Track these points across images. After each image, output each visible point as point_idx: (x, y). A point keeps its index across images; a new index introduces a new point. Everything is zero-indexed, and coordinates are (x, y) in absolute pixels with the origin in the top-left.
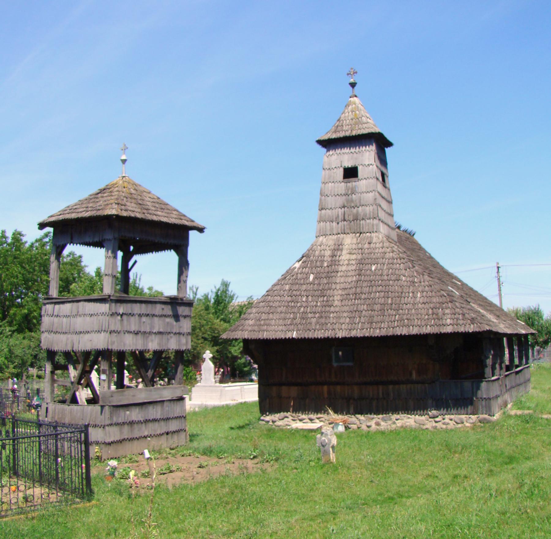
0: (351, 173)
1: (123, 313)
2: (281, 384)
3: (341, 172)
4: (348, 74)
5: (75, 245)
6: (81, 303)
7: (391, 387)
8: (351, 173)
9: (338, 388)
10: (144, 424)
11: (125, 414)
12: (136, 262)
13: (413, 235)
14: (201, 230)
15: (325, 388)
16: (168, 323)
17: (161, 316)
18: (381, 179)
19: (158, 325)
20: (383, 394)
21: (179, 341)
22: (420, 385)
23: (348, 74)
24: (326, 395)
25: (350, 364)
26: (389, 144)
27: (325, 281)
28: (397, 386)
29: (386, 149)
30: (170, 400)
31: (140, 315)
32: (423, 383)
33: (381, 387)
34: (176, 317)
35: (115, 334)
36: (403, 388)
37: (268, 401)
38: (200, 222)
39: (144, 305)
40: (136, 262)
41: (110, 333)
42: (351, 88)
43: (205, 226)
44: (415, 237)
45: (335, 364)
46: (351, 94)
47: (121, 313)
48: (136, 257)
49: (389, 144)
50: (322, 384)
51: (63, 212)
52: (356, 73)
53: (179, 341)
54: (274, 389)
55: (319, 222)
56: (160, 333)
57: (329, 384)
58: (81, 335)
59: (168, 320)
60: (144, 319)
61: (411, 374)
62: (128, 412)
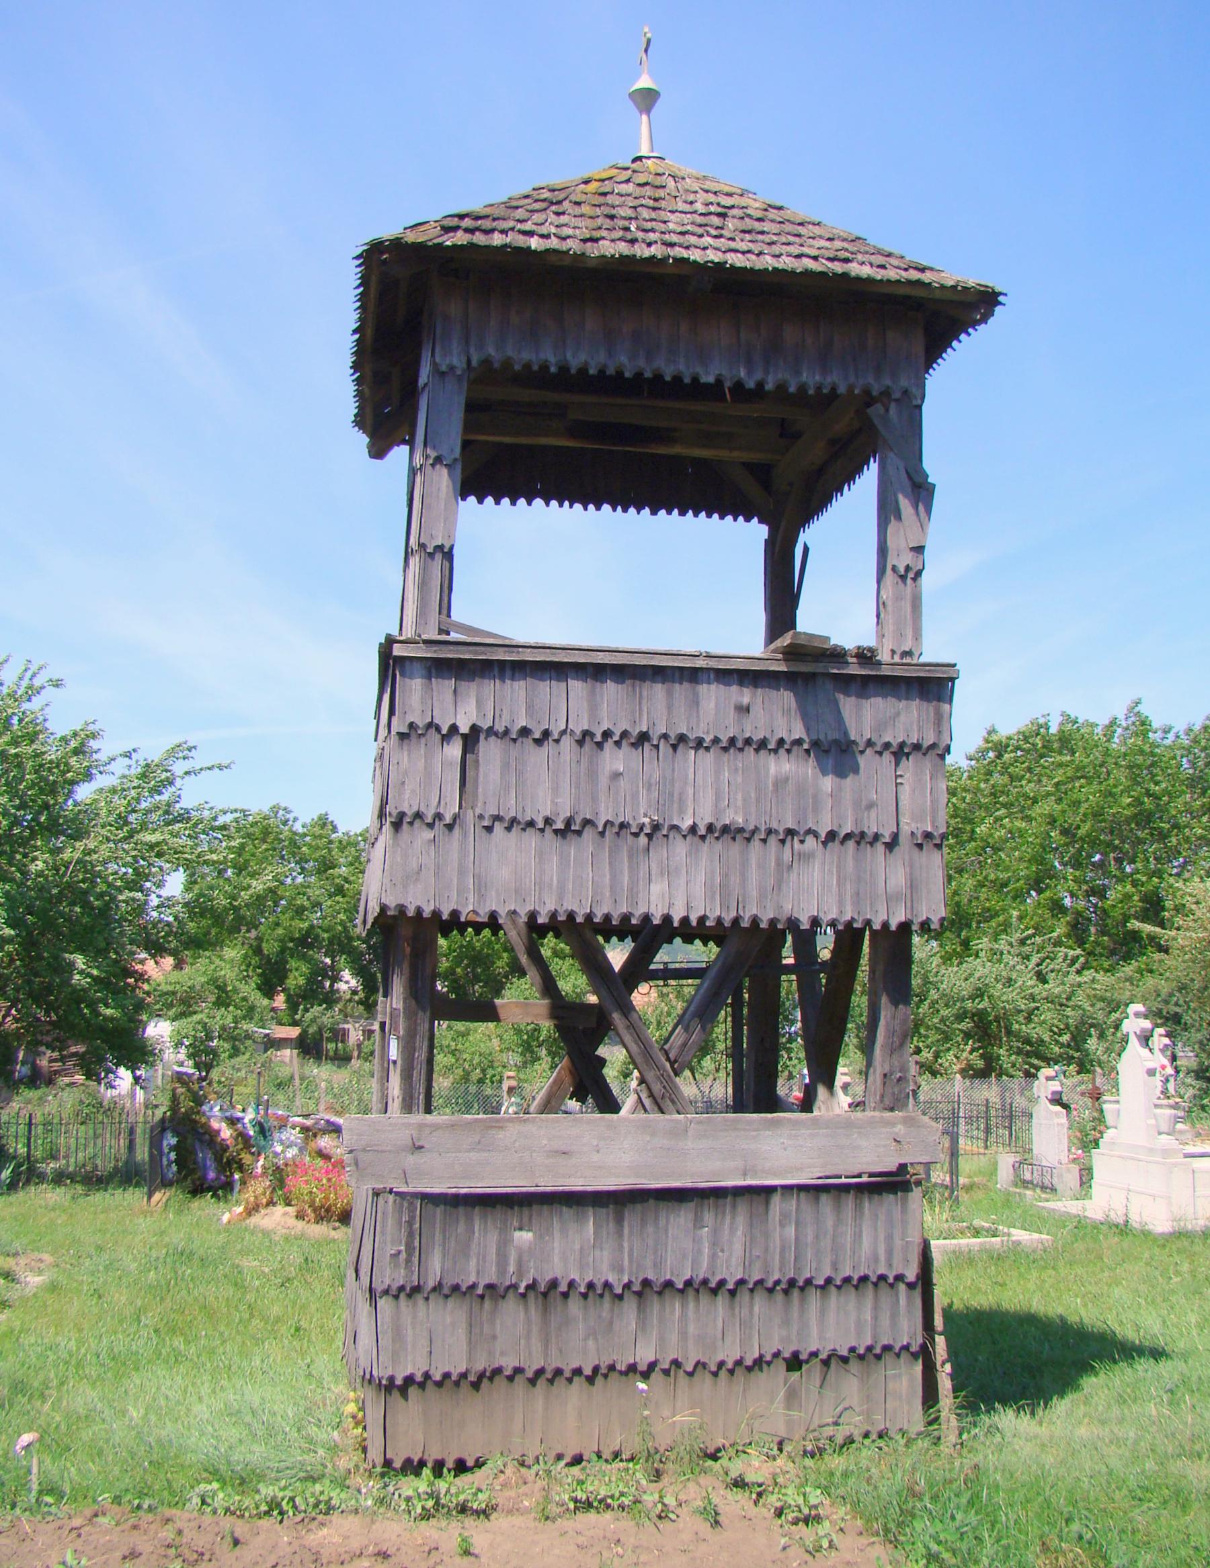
1: (475, 729)
5: (522, 502)
10: (630, 1306)
11: (504, 1244)
12: (806, 550)
16: (781, 783)
19: (707, 789)
30: (814, 1190)
34: (836, 753)
35: (428, 834)
39: (610, 689)
40: (806, 550)
47: (464, 729)
59: (778, 766)
60: (615, 759)
62: (524, 1237)
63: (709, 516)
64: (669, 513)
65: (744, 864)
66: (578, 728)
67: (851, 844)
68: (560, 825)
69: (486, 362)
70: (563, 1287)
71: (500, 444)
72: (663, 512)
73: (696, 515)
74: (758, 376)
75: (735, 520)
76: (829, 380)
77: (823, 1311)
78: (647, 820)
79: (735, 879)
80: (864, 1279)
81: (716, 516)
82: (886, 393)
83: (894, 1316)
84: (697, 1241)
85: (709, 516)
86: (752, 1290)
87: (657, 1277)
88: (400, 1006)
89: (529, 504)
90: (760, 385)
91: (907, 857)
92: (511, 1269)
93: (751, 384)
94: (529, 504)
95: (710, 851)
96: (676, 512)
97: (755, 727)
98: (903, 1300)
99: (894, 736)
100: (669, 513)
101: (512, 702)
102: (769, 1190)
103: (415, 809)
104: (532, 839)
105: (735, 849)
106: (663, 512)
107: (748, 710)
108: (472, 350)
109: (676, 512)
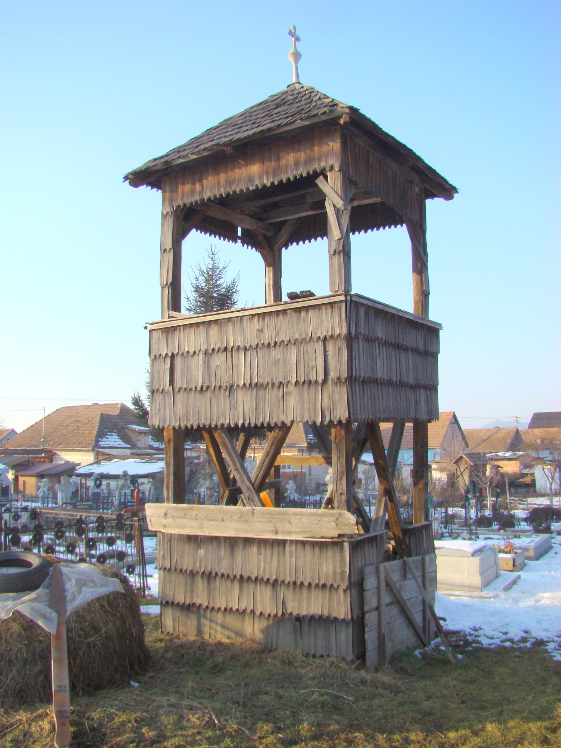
16: (276, 362)
30: (303, 543)
47: (170, 355)
63: (390, 227)
64: (372, 230)
67: (306, 386)
68: (199, 389)
70: (214, 574)
71: (299, 218)
72: (370, 231)
73: (384, 229)
74: (271, 180)
75: (402, 226)
76: (299, 172)
77: (308, 598)
78: (228, 384)
80: (324, 586)
81: (393, 227)
82: (324, 169)
83: (339, 603)
84: (259, 561)
85: (390, 227)
86: (281, 586)
87: (246, 575)
89: (316, 240)
90: (273, 183)
91: (330, 390)
92: (198, 565)
93: (268, 185)
94: (316, 240)
96: (375, 229)
97: (266, 338)
98: (342, 598)
99: (321, 333)
100: (372, 230)
102: (283, 543)
103: (157, 388)
106: (370, 231)
107: (262, 330)
108: (174, 203)
109: (375, 229)
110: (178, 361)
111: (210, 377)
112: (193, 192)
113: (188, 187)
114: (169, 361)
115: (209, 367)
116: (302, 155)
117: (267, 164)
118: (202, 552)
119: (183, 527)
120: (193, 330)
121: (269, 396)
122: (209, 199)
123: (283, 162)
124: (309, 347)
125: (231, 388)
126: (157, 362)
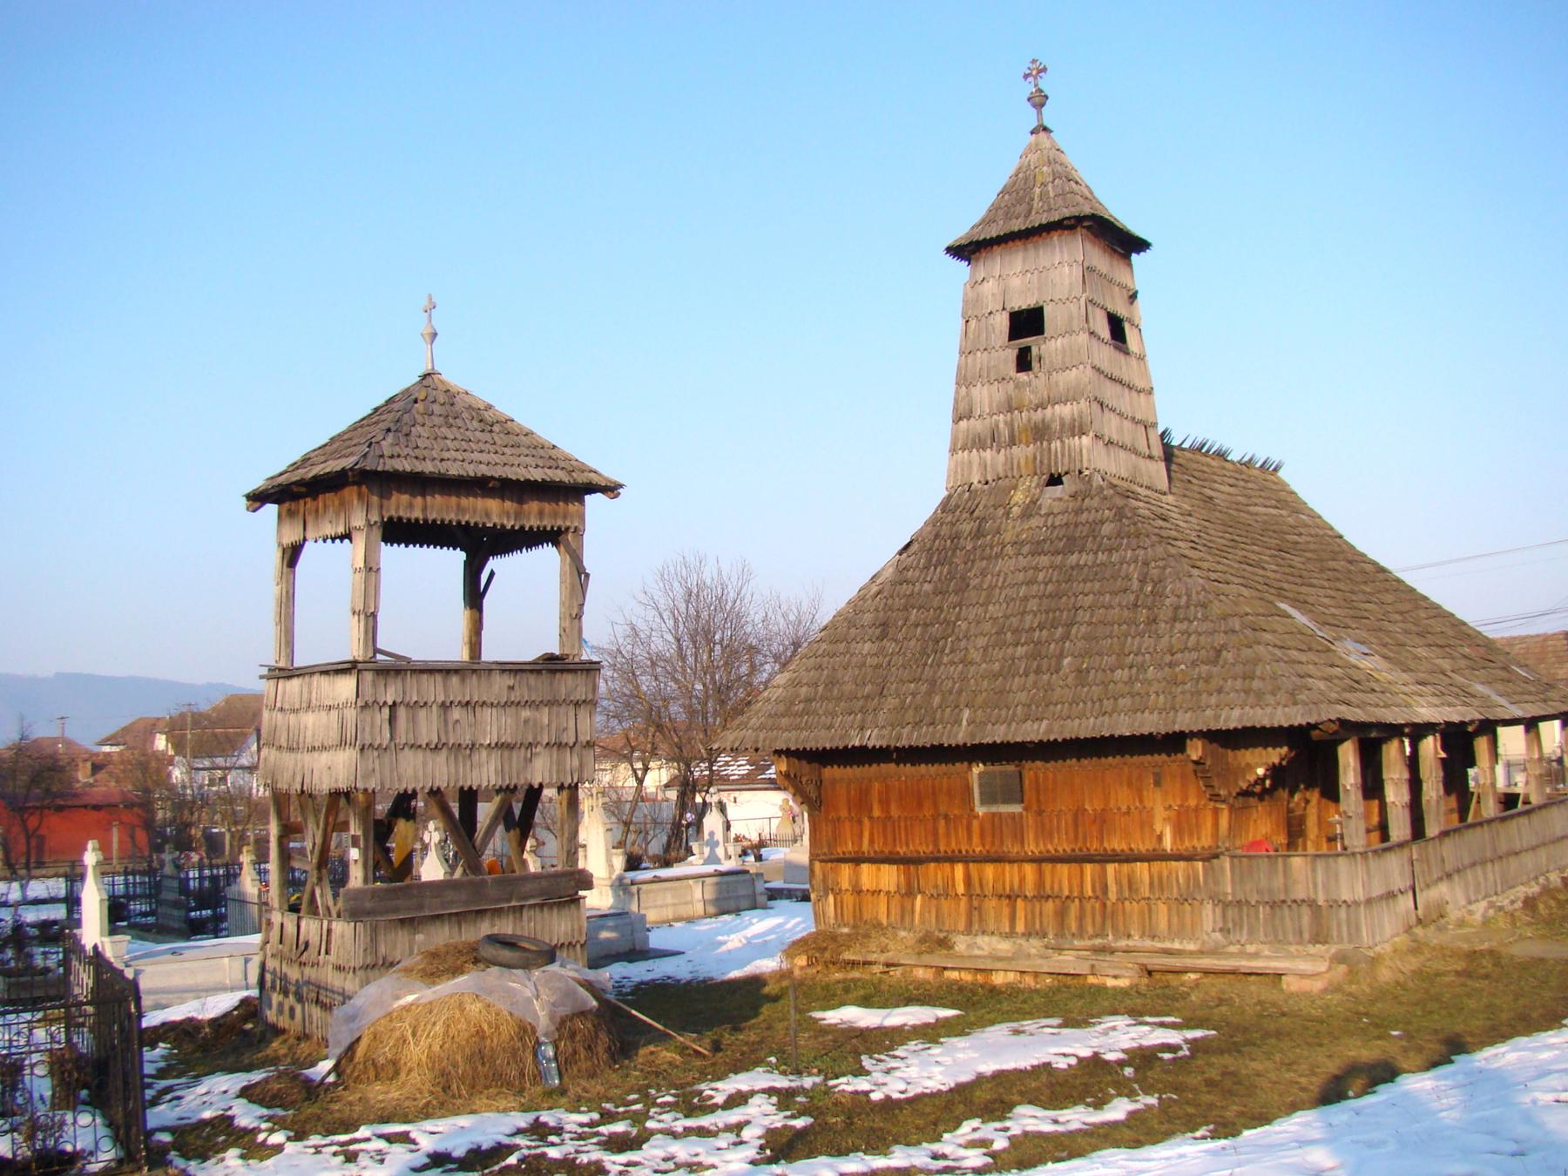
0: (1027, 323)
2: (857, 860)
3: (1002, 322)
4: (1026, 76)
6: (316, 678)
7: (1111, 868)
8: (1027, 323)
9: (989, 870)
12: (492, 574)
13: (1276, 470)
14: (611, 489)
15: (959, 869)
16: (526, 722)
17: (507, 704)
18: (1105, 333)
20: (1094, 890)
21: (560, 763)
22: (1182, 864)
23: (1026, 76)
24: (961, 889)
25: (1016, 809)
26: (1141, 245)
27: (953, 598)
28: (1125, 867)
29: (1134, 256)
31: (445, 707)
32: (1189, 858)
33: (1088, 868)
36: (1141, 869)
37: (831, 898)
38: (608, 470)
40: (492, 574)
41: (362, 749)
42: (1034, 111)
43: (621, 481)
44: (1281, 474)
45: (980, 810)
46: (1035, 124)
47: (390, 702)
48: (494, 563)
49: (1141, 245)
50: (952, 859)
51: (295, 466)
52: (1044, 70)
53: (560, 763)
54: (846, 870)
55: (953, 451)
56: (500, 746)
57: (966, 860)
58: (316, 754)
61: (1160, 838)
65: (510, 759)
66: (441, 698)
69: (391, 518)
79: (507, 768)
82: (567, 529)
88: (359, 833)
95: (496, 754)
101: (417, 689)
104: (420, 754)
105: (506, 753)
110: (402, 713)
111: (447, 733)
112: (411, 506)
113: (405, 498)
114: (386, 711)
115: (446, 721)
116: (547, 507)
117: (508, 504)
118: (420, 937)
119: (396, 910)
120: (425, 676)
121: (518, 756)
122: (434, 521)
123: (525, 507)
124: (563, 709)
125: (472, 747)
126: (367, 714)
